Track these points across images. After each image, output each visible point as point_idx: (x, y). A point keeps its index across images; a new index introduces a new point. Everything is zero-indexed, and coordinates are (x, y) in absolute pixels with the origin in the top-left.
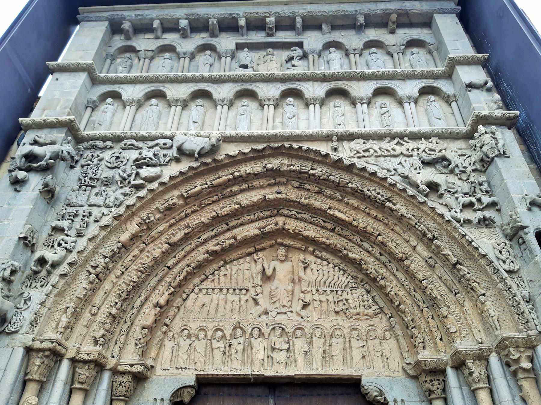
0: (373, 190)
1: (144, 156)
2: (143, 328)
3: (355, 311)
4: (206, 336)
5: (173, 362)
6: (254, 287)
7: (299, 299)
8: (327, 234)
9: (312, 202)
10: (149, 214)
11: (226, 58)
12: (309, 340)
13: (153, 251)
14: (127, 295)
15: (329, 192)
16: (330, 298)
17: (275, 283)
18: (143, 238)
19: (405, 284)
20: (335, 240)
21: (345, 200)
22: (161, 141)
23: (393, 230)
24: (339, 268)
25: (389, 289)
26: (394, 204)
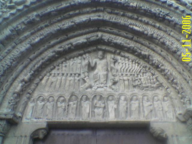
0: (158, 10)
2: (14, 93)
3: (145, 85)
5: (33, 114)
6: (84, 73)
7: (111, 80)
8: (128, 41)
10: (18, 25)
12: (117, 102)
13: (20, 48)
14: (4, 73)
15: (130, 14)
16: (130, 78)
17: (96, 71)
18: (14, 40)
19: (177, 67)
20: (132, 45)
21: (140, 18)
23: (169, 35)
24: (135, 62)
25: (167, 71)
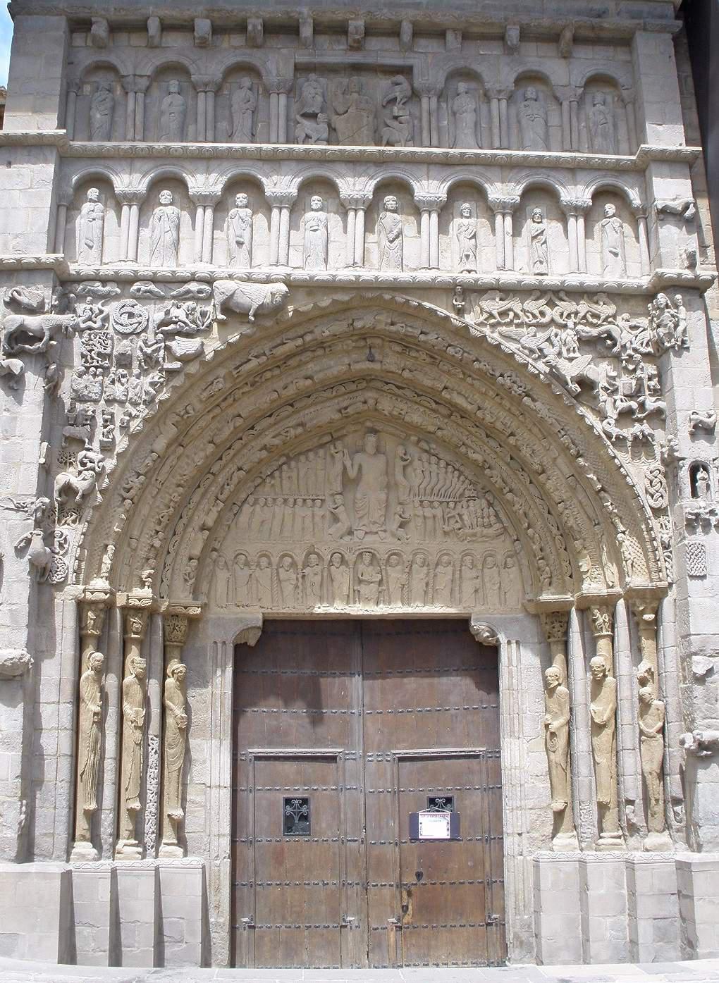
1: (174, 319)
2: (191, 559)
4: (270, 564)
5: (230, 596)
9: (419, 377)
11: (278, 94)
12: (407, 570)
16: (439, 512)
22: (194, 287)
23: (530, 430)
25: (517, 506)
26: (534, 400)
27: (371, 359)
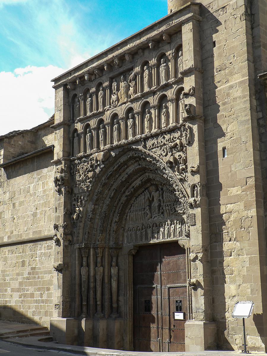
27: (139, 165)
